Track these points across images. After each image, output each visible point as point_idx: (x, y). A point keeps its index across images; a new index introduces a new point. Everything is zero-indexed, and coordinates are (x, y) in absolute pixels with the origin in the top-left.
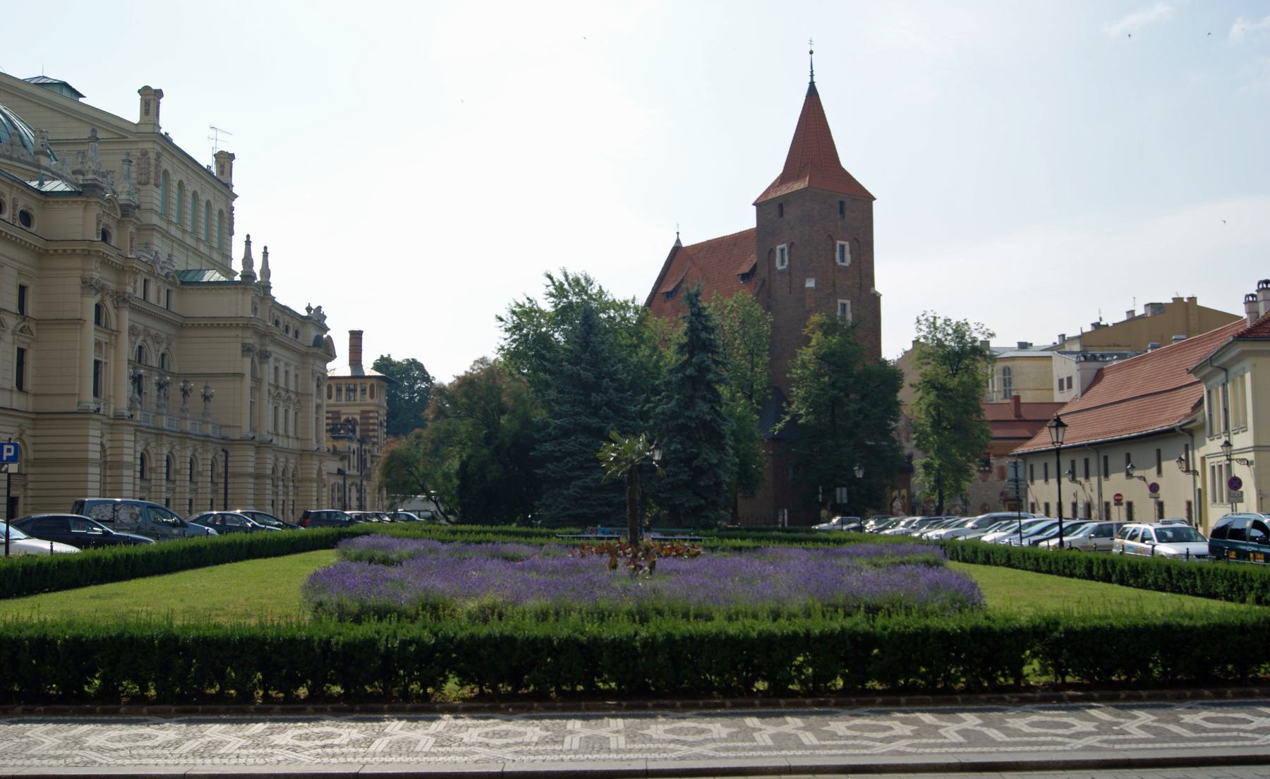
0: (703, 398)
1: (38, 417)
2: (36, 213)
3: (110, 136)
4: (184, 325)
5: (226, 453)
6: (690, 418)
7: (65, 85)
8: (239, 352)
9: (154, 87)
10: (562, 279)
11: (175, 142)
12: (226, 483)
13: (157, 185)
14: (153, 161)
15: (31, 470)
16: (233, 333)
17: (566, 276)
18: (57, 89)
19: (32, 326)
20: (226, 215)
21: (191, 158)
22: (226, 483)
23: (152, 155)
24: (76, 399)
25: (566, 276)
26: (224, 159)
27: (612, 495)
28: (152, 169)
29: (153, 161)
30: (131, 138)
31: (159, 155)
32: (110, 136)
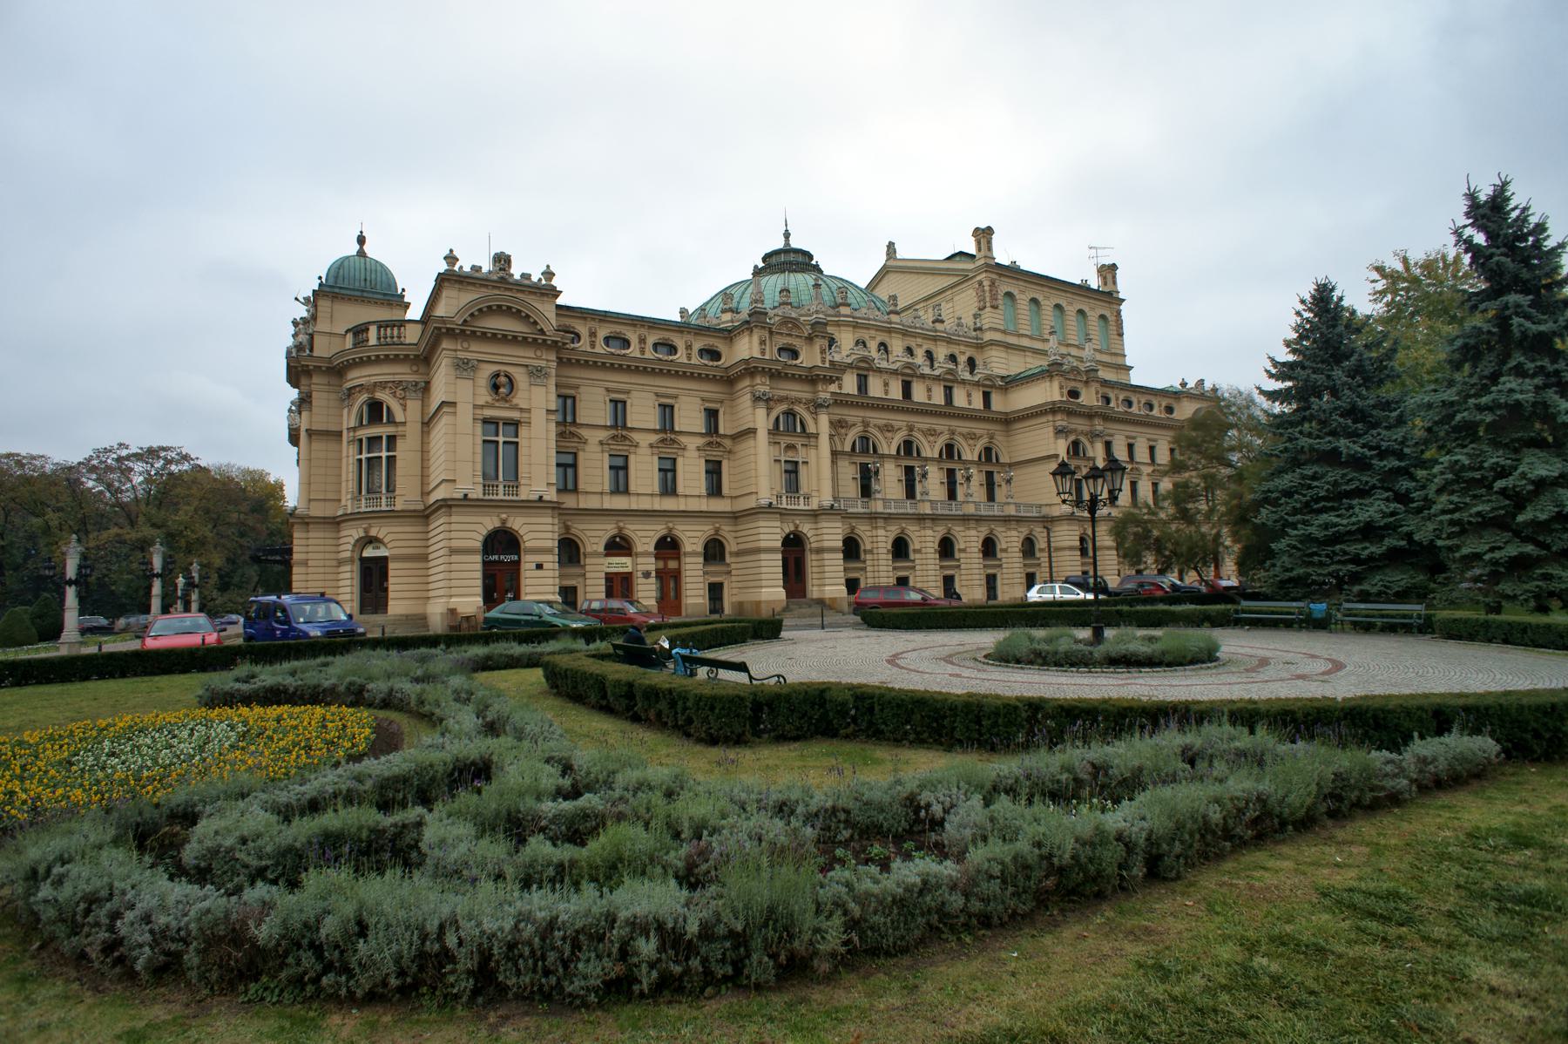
0: (1519, 371)
1: (736, 517)
2: (720, 346)
3: (956, 279)
4: (1008, 421)
5: (1048, 530)
6: (1480, 408)
7: (961, 253)
8: (1052, 434)
9: (983, 226)
10: (1399, 267)
11: (1024, 267)
12: (1050, 557)
13: (995, 307)
14: (987, 288)
15: (733, 560)
16: (1044, 419)
17: (1405, 261)
18: (958, 258)
19: (727, 443)
20: (1111, 318)
21: (1047, 278)
22: (1050, 557)
23: (986, 283)
24: (754, 496)
25: (1405, 261)
26: (1108, 271)
27: (1359, 546)
28: (987, 294)
29: (987, 288)
30: (971, 275)
31: (993, 284)
32: (956, 279)
